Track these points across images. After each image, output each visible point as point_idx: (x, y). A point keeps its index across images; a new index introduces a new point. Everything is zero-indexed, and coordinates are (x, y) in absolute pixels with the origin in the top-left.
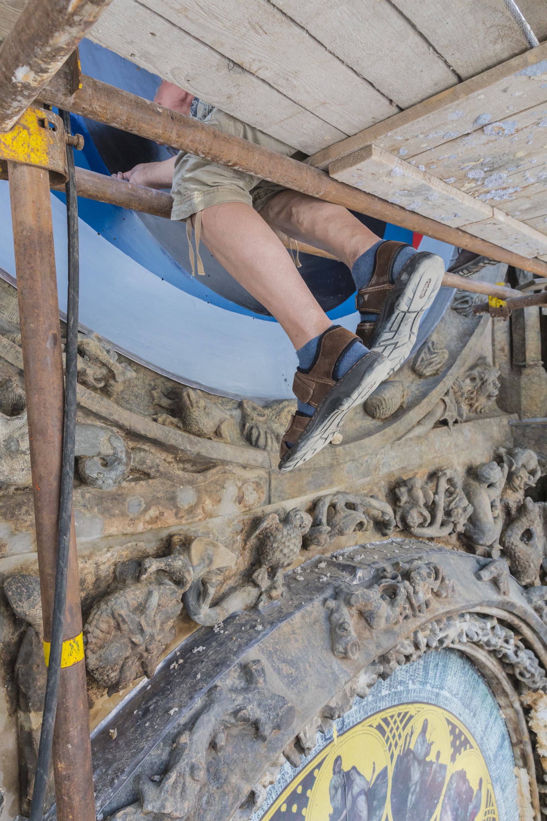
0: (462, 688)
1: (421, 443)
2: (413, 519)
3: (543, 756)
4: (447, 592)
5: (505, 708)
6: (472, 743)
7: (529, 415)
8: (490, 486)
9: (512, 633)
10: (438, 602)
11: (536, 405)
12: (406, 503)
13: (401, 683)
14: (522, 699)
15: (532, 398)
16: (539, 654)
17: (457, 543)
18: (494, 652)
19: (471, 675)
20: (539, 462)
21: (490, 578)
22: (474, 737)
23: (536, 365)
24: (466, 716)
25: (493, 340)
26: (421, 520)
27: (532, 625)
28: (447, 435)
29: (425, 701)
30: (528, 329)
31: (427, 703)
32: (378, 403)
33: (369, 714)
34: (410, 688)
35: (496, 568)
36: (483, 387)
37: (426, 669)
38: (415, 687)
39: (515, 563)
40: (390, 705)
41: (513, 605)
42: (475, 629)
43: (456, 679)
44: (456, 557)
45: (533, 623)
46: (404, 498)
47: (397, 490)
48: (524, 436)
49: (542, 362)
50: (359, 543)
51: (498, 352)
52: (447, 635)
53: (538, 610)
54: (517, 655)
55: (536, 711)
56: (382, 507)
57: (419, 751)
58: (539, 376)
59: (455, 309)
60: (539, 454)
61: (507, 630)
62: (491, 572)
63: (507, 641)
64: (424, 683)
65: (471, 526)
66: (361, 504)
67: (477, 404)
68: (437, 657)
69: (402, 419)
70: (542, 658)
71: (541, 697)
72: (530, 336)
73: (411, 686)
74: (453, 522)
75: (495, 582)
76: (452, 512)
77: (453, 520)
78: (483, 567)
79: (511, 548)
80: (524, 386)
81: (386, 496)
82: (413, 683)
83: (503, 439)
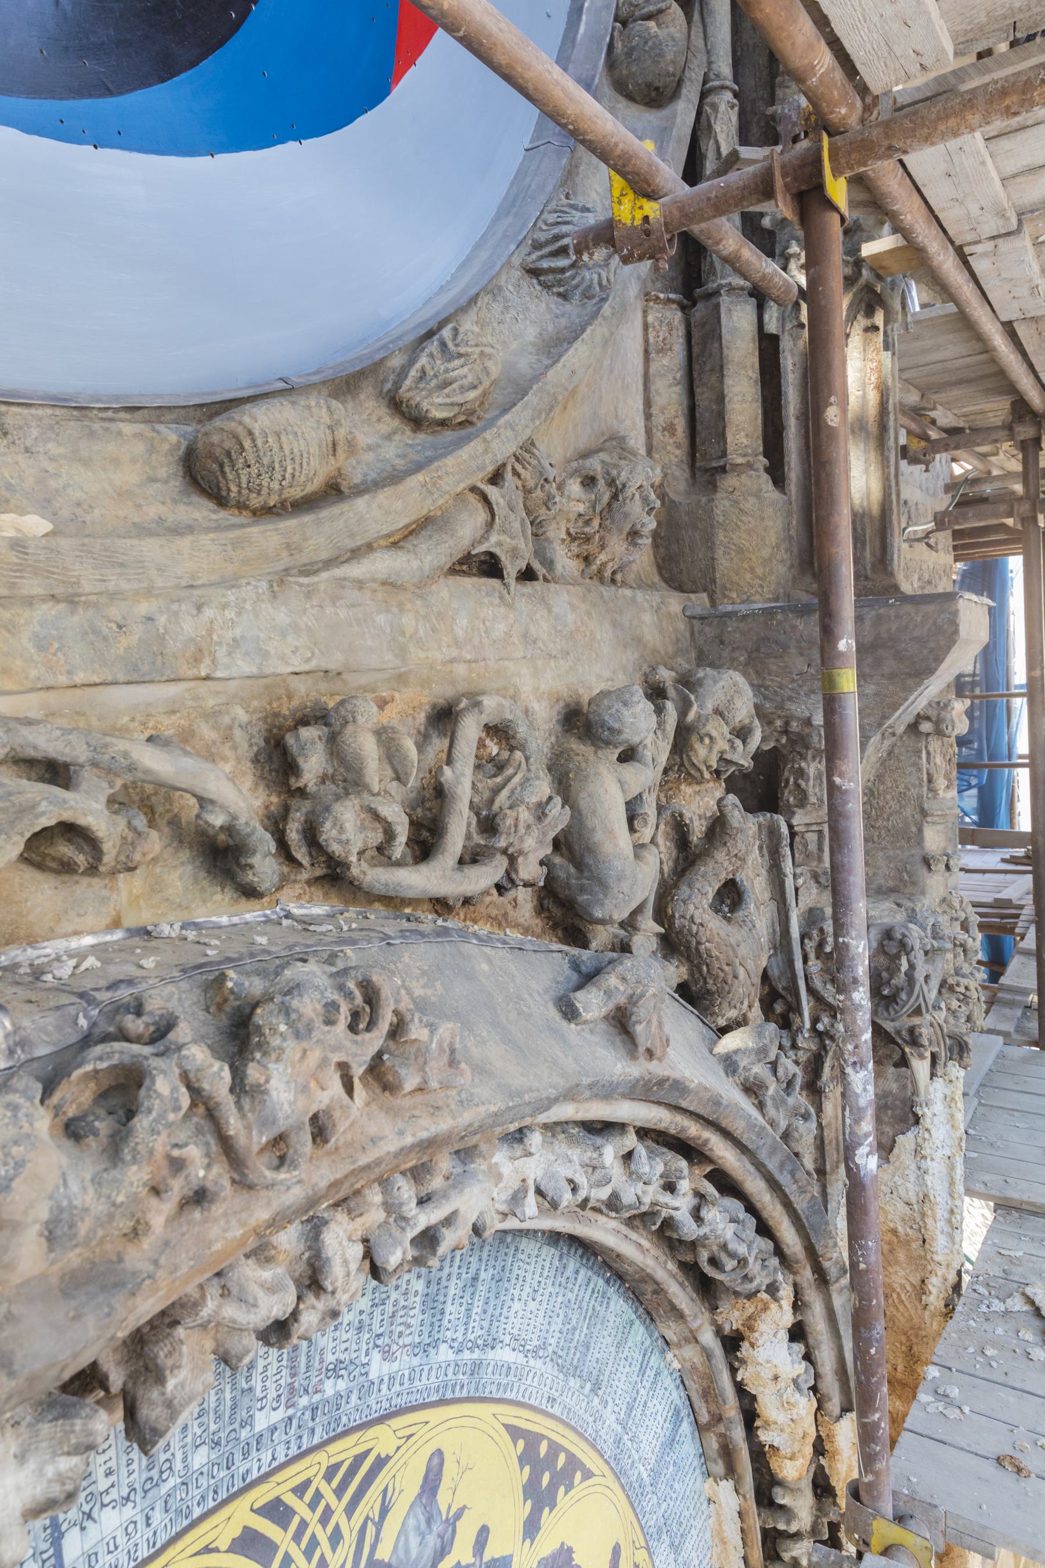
0: (557, 1324)
1: (401, 606)
2: (342, 830)
3: (771, 1446)
4: (422, 1069)
5: (679, 1346)
6: (589, 1464)
7: (734, 595)
8: (628, 755)
9: (683, 1164)
10: (389, 1110)
11: (752, 570)
12: (323, 779)
13: (335, 1371)
14: (720, 1320)
15: (741, 551)
16: (759, 1205)
17: (537, 923)
18: (642, 1219)
19: (584, 1282)
20: (759, 711)
21: (604, 1011)
22: (593, 1447)
23: (750, 466)
24: (573, 1398)
25: (648, 403)
26: (376, 837)
27: (737, 1134)
28: (498, 601)
29: (434, 1398)
30: (730, 370)
31: (442, 1402)
32: (227, 445)
33: (197, 1512)
34: (373, 1375)
35: (624, 979)
36: (615, 505)
37: (433, 1304)
38: (395, 1366)
39: (700, 971)
40: (294, 1451)
41: (679, 1086)
42: (565, 1171)
43: (541, 1302)
44: (499, 955)
45: (738, 1127)
46: (313, 765)
47: (290, 740)
48: (722, 642)
49: (765, 461)
50: (131, 920)
51: (658, 435)
52: (455, 1213)
53: (752, 1089)
54: (698, 1218)
55: (752, 1345)
56: (237, 797)
57: (414, 1553)
58: (758, 495)
59: (534, 272)
60: (757, 688)
61: (670, 1155)
62: (608, 993)
63: (670, 1187)
64: (425, 1349)
65: (572, 870)
66: (95, 764)
67: (602, 557)
68: (474, 1259)
69: (325, 513)
70: (765, 1214)
71: (766, 1308)
72: (736, 390)
73: (378, 1367)
74: (504, 852)
75: (621, 1023)
76: (498, 820)
77: (502, 843)
78: (587, 978)
79: (690, 931)
80: (721, 519)
81: (256, 760)
82: (387, 1355)
83: (671, 649)
